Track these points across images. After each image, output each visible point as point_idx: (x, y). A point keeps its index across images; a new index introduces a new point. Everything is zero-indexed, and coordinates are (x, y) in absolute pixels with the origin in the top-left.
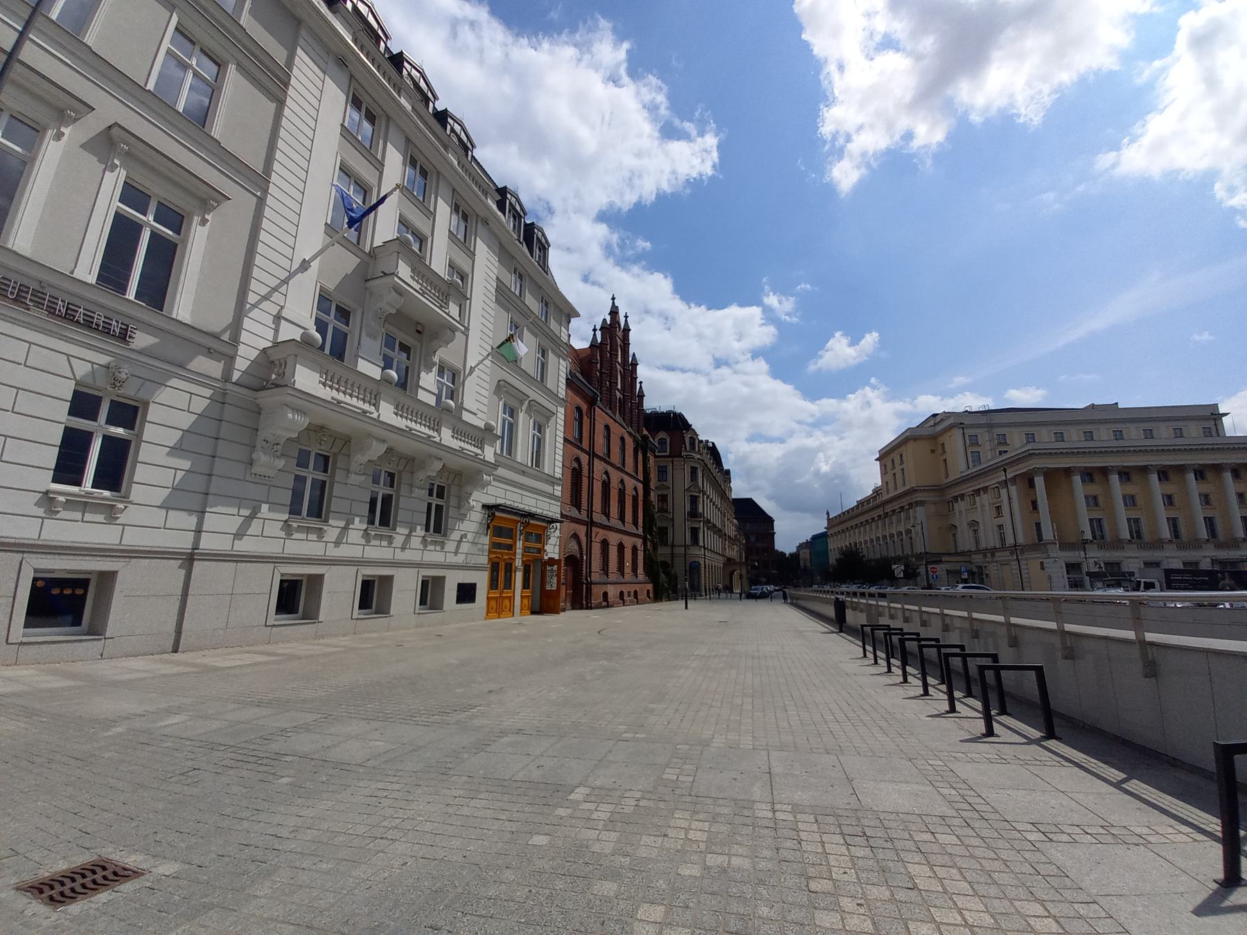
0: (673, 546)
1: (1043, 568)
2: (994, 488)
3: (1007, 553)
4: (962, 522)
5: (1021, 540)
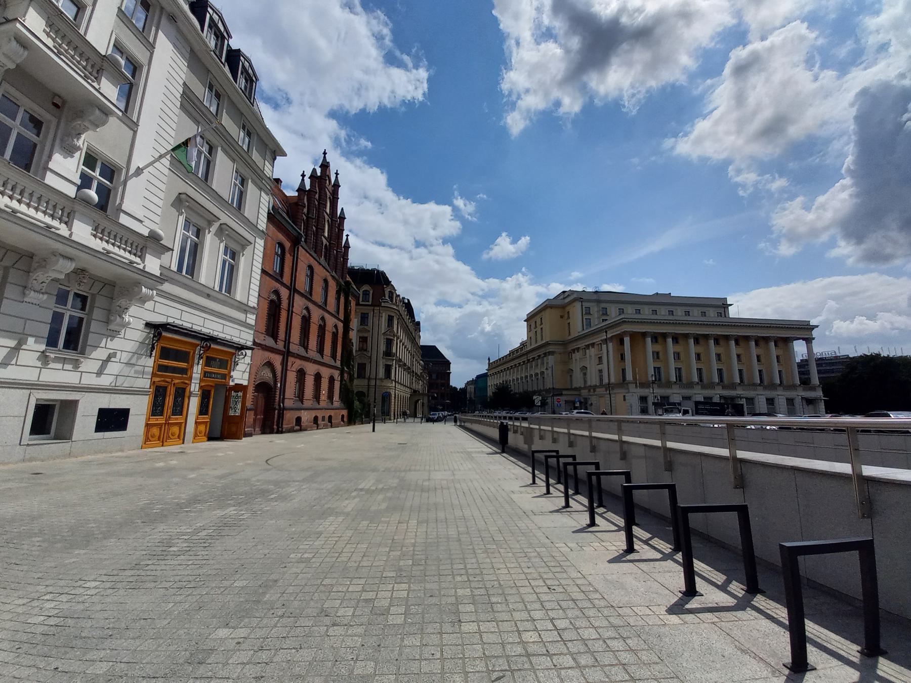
0: (369, 379)
1: (625, 400)
2: (598, 344)
3: (604, 389)
4: (576, 368)
5: (613, 380)
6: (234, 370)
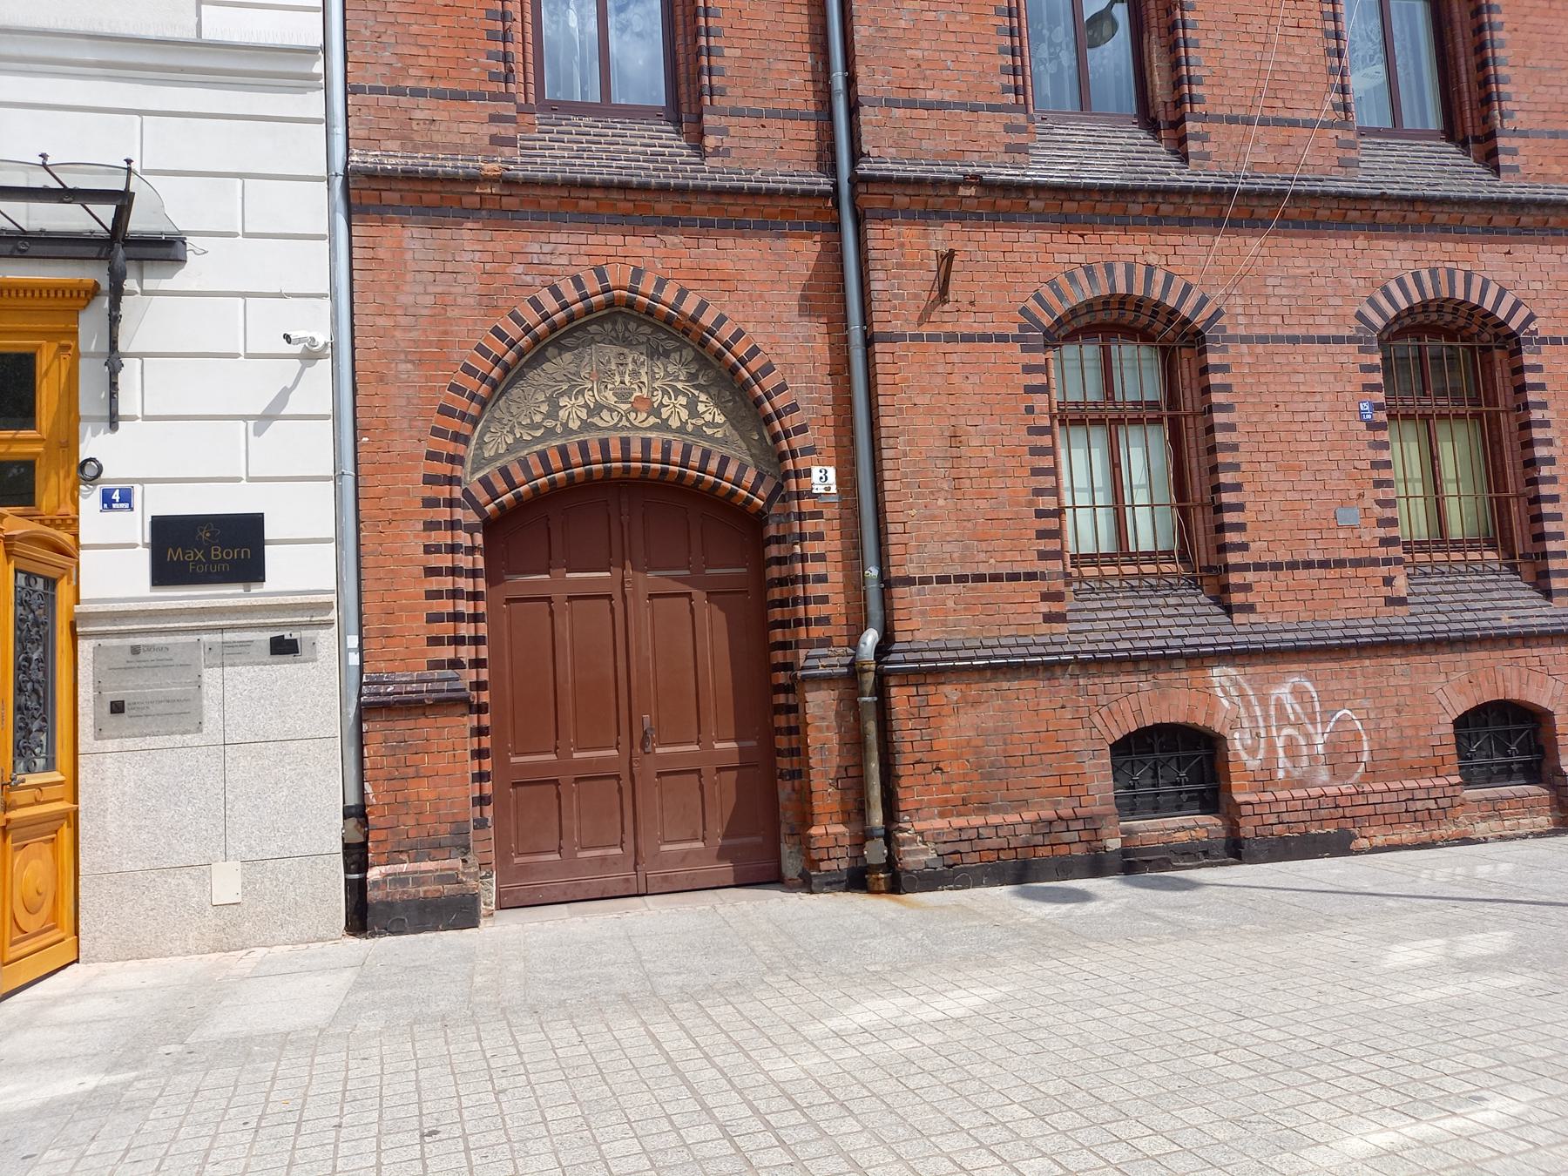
6: (113, 421)
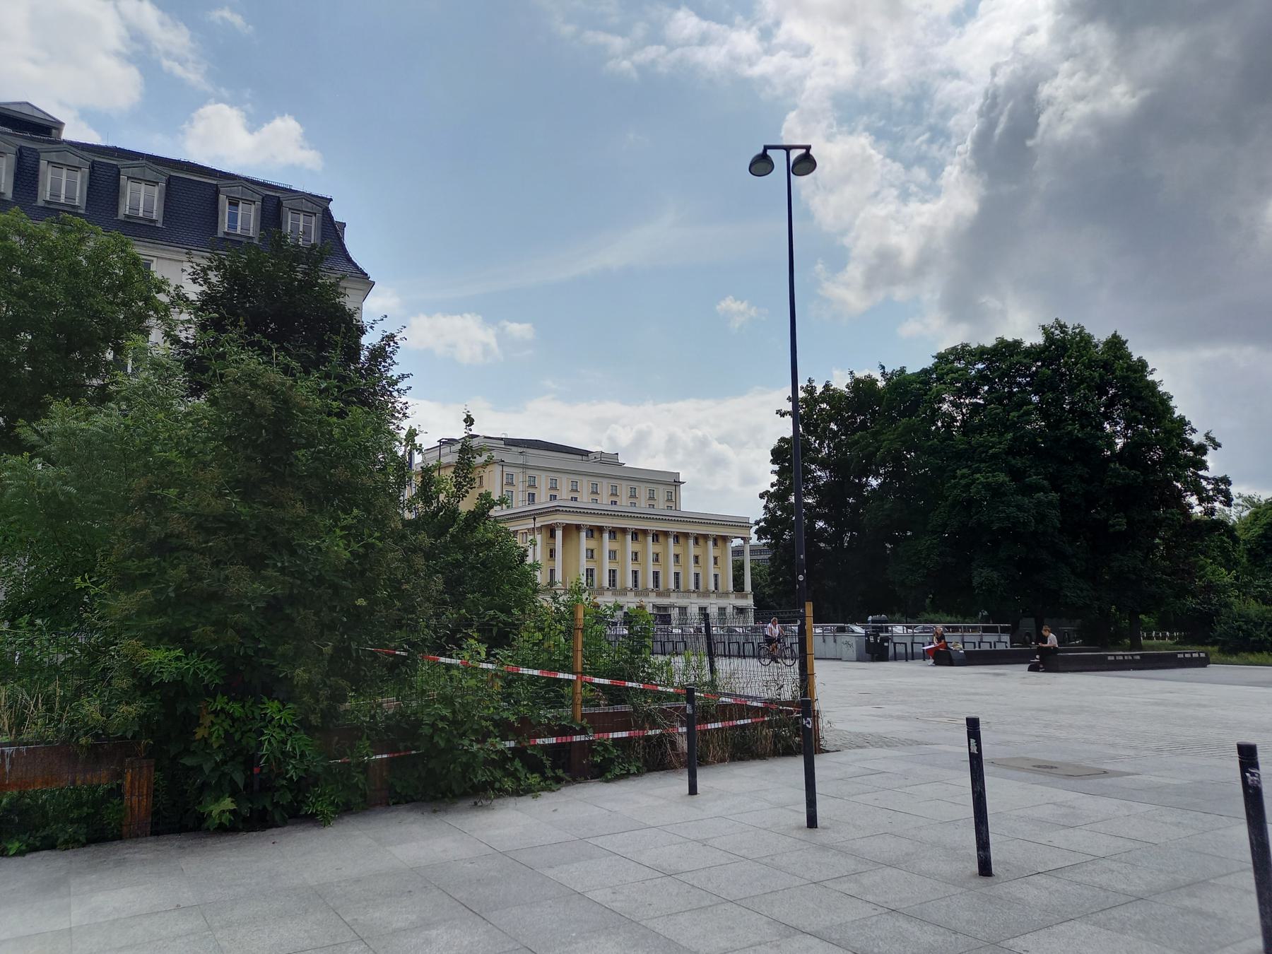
2: (523, 533)
